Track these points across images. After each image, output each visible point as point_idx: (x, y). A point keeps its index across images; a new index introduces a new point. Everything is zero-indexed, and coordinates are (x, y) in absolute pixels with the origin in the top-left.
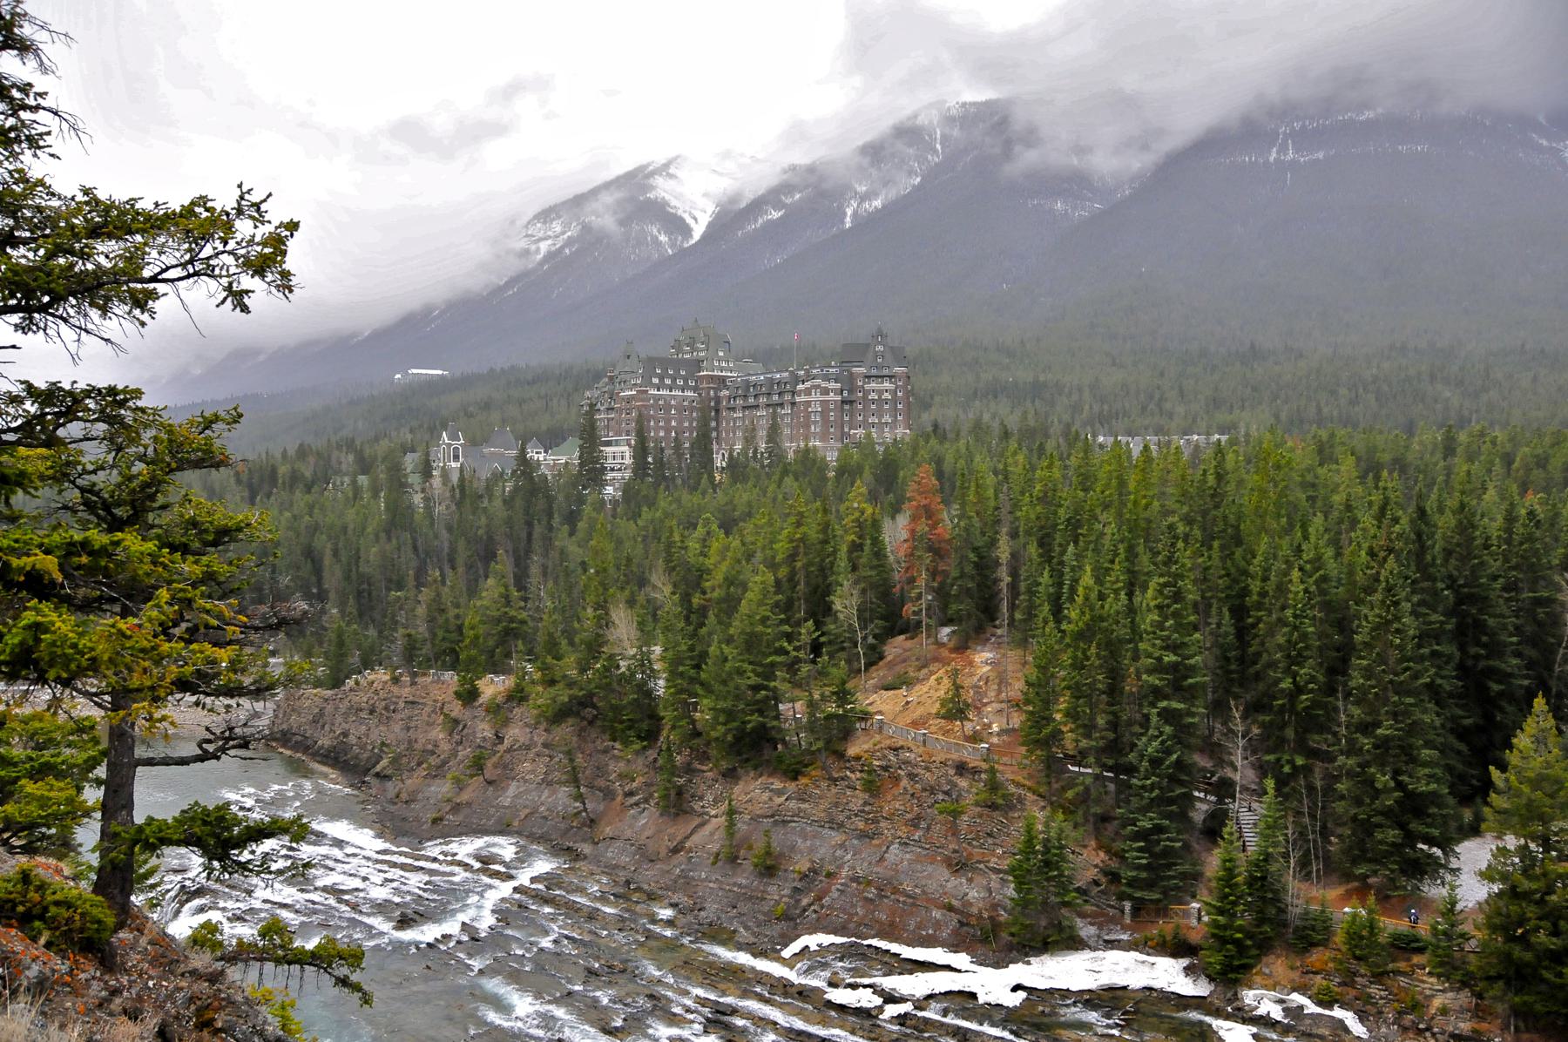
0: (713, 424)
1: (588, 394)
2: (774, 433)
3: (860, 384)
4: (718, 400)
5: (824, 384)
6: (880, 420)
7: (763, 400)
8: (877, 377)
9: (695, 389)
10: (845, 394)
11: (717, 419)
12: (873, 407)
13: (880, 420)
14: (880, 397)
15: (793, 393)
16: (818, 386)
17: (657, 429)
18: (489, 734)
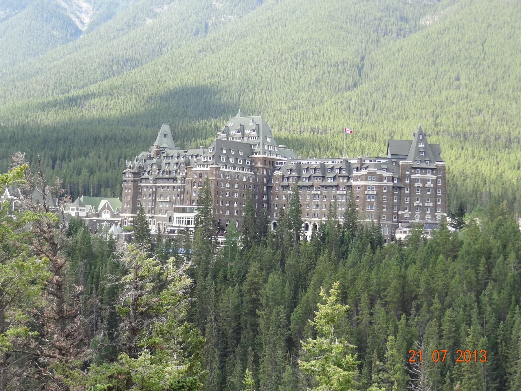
0: (265, 198)
1: (130, 164)
3: (408, 173)
4: (270, 178)
8: (422, 169)
9: (252, 168)
10: (396, 182)
11: (268, 195)
12: (418, 193)
14: (424, 185)
15: (349, 178)
16: (374, 174)
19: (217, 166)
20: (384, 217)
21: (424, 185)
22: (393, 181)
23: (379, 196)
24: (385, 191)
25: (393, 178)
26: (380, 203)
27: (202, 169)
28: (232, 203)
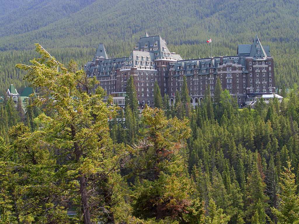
12: (258, 76)
14: (261, 71)
16: (230, 66)
17: (141, 88)
19: (135, 68)
20: (238, 92)
21: (261, 71)
27: (126, 70)
28: (145, 89)
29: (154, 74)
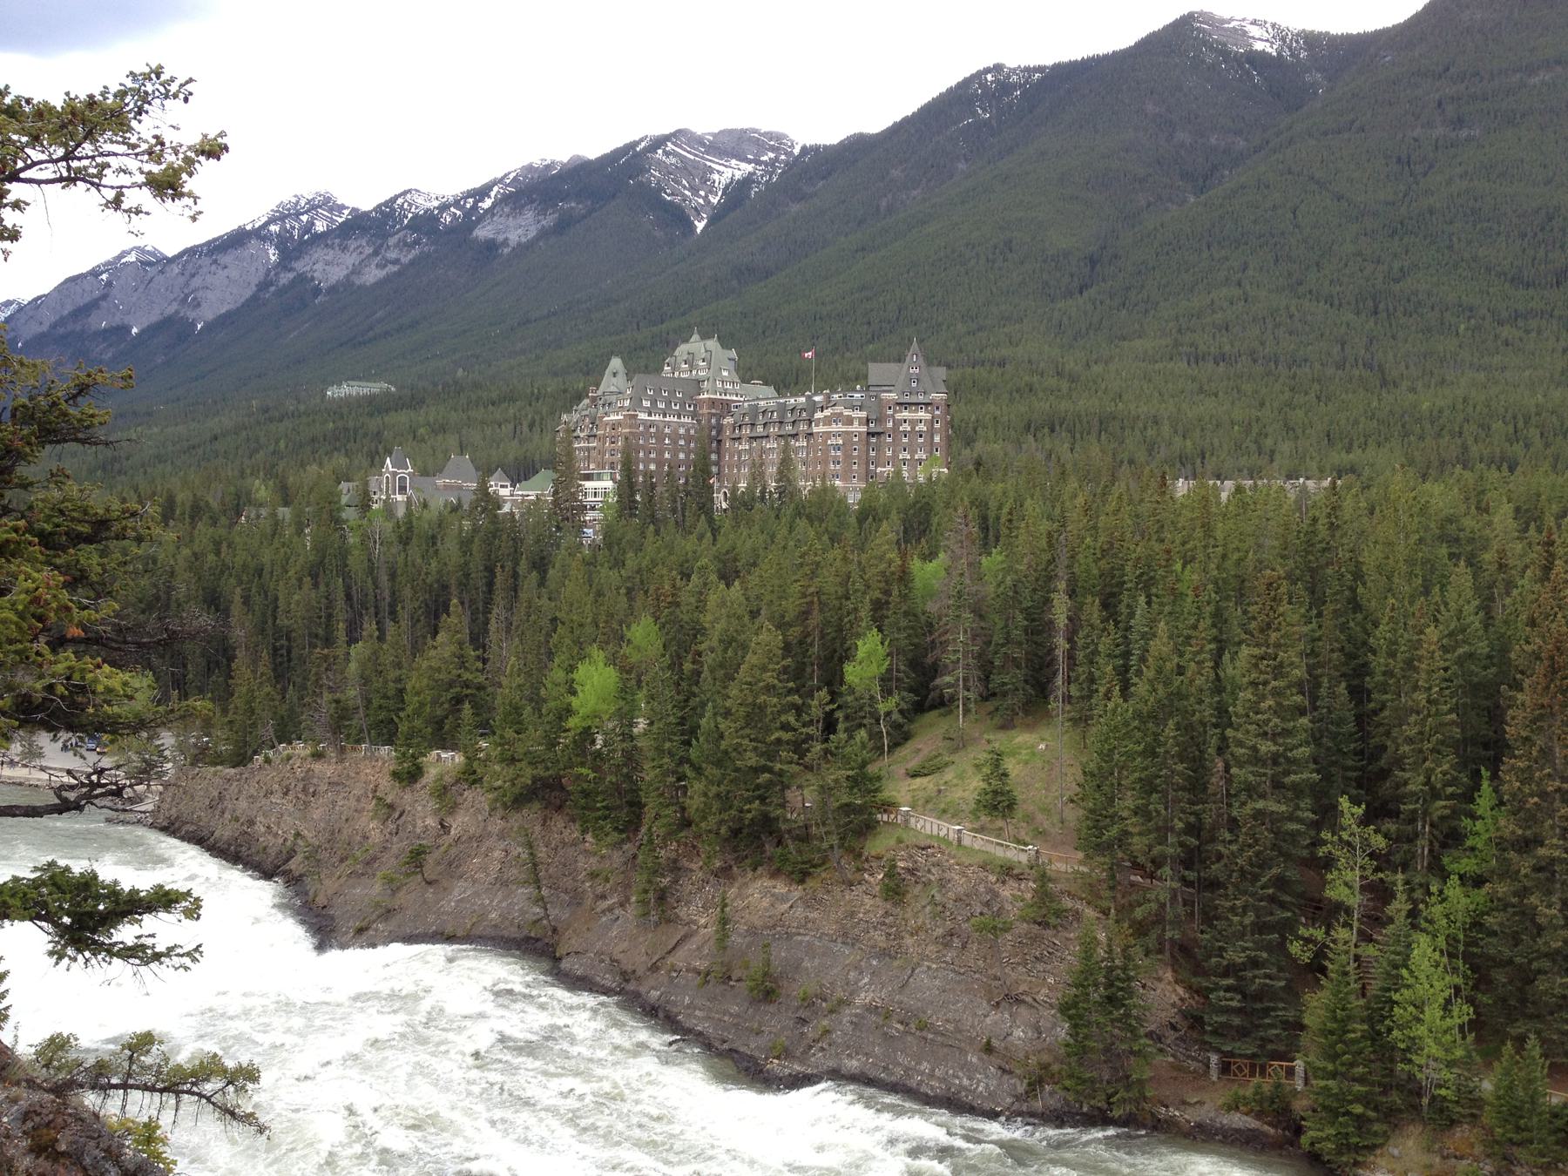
0: (714, 457)
1: (565, 417)
2: (786, 463)
4: (720, 428)
5: (847, 413)
6: (913, 456)
7: (773, 430)
9: (694, 415)
11: (718, 452)
12: (905, 440)
13: (913, 456)
14: (913, 429)
17: (647, 461)
18: (431, 822)
21: (913, 429)
22: (868, 425)
23: (846, 447)
24: (856, 439)
25: (868, 420)
26: (848, 456)
29: (688, 431)
